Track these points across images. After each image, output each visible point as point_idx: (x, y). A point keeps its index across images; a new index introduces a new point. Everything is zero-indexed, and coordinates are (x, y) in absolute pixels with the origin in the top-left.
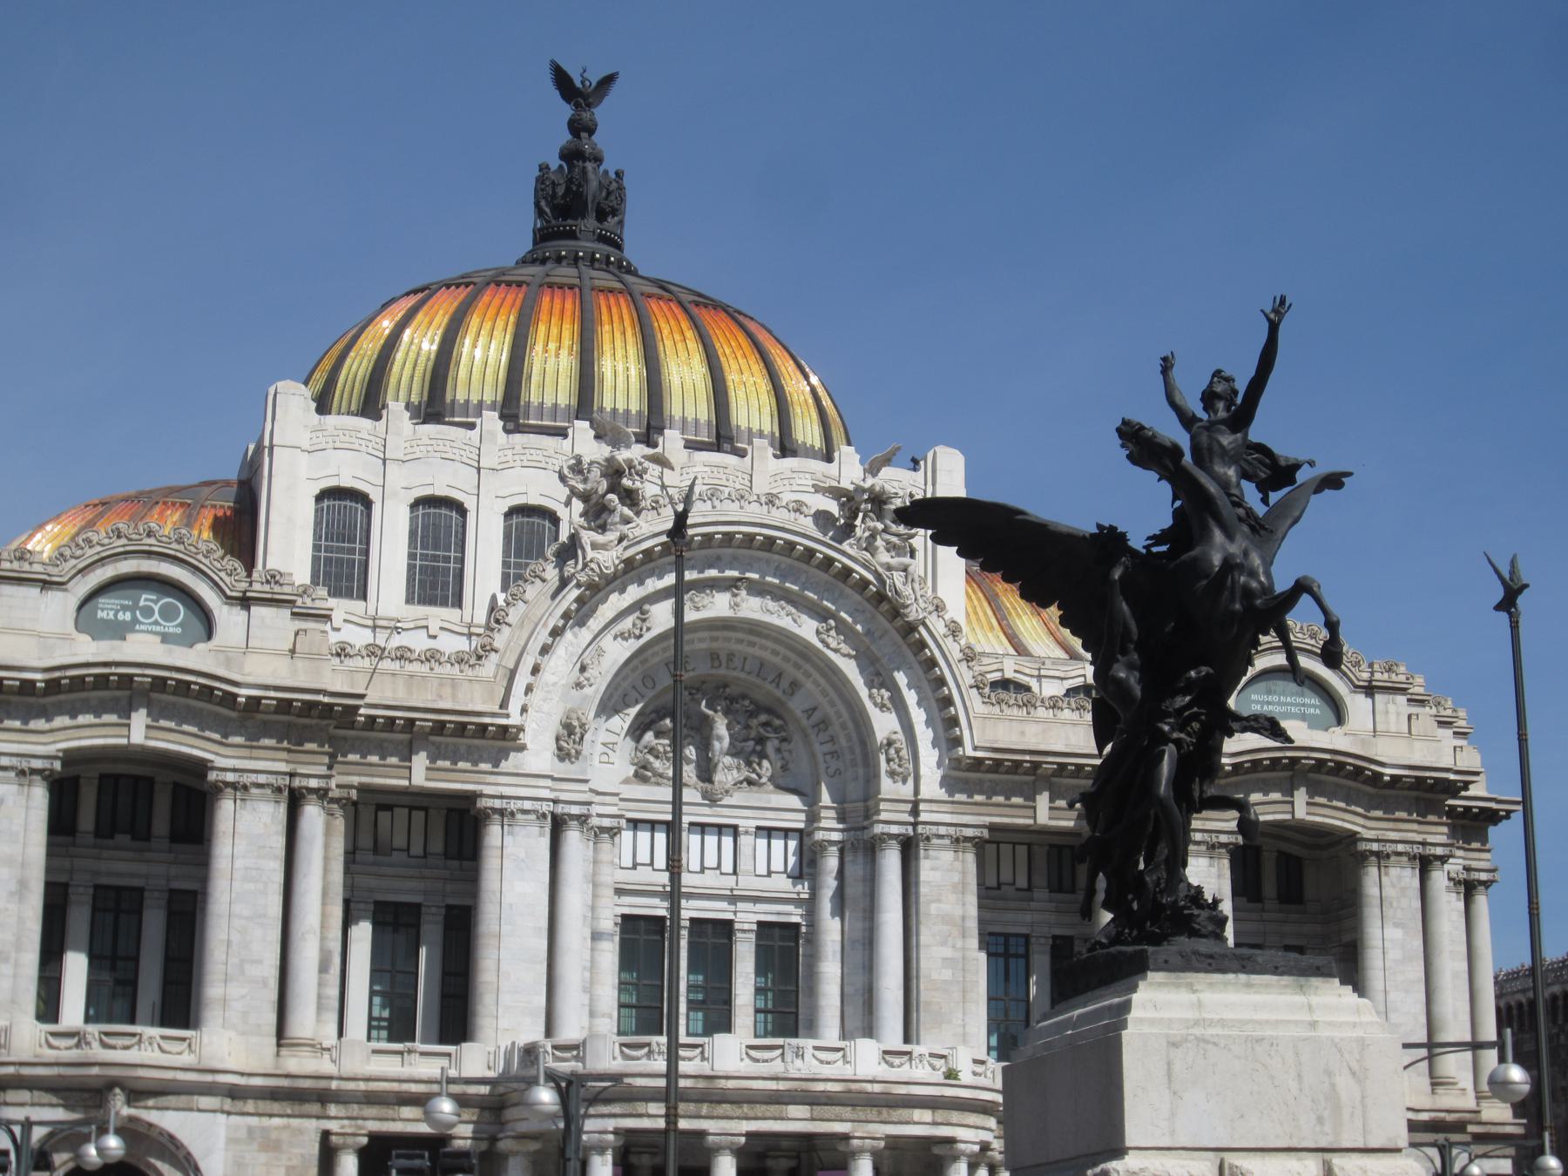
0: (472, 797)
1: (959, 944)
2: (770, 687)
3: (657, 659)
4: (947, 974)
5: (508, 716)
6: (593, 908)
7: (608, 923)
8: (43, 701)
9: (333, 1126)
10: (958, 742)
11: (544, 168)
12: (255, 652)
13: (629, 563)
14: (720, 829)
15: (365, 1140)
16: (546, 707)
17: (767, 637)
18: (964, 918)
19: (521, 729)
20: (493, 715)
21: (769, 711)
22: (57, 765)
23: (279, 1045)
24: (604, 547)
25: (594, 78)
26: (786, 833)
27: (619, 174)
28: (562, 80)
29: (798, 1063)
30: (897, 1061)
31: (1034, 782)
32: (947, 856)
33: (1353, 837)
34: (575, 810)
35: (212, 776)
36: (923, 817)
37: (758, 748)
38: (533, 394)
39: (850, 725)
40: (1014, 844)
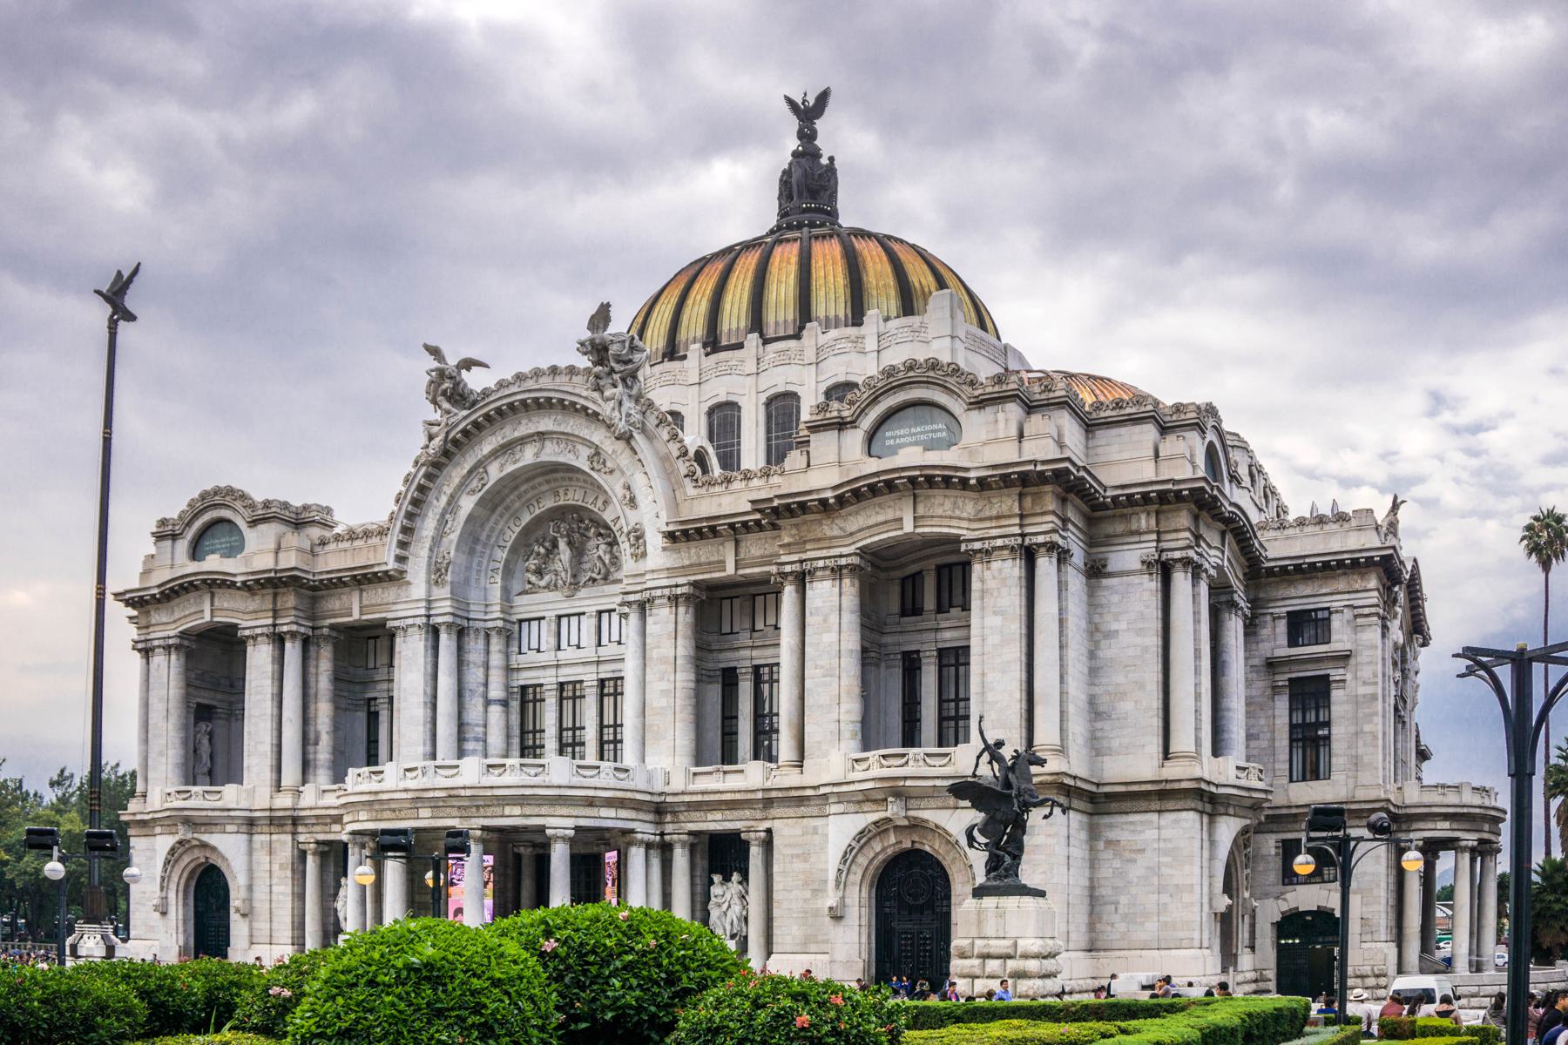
3: (517, 505)
4: (663, 702)
14: (579, 614)
27: (831, 159)
30: (496, 772)
33: (956, 540)
34: (440, 620)
38: (682, 335)
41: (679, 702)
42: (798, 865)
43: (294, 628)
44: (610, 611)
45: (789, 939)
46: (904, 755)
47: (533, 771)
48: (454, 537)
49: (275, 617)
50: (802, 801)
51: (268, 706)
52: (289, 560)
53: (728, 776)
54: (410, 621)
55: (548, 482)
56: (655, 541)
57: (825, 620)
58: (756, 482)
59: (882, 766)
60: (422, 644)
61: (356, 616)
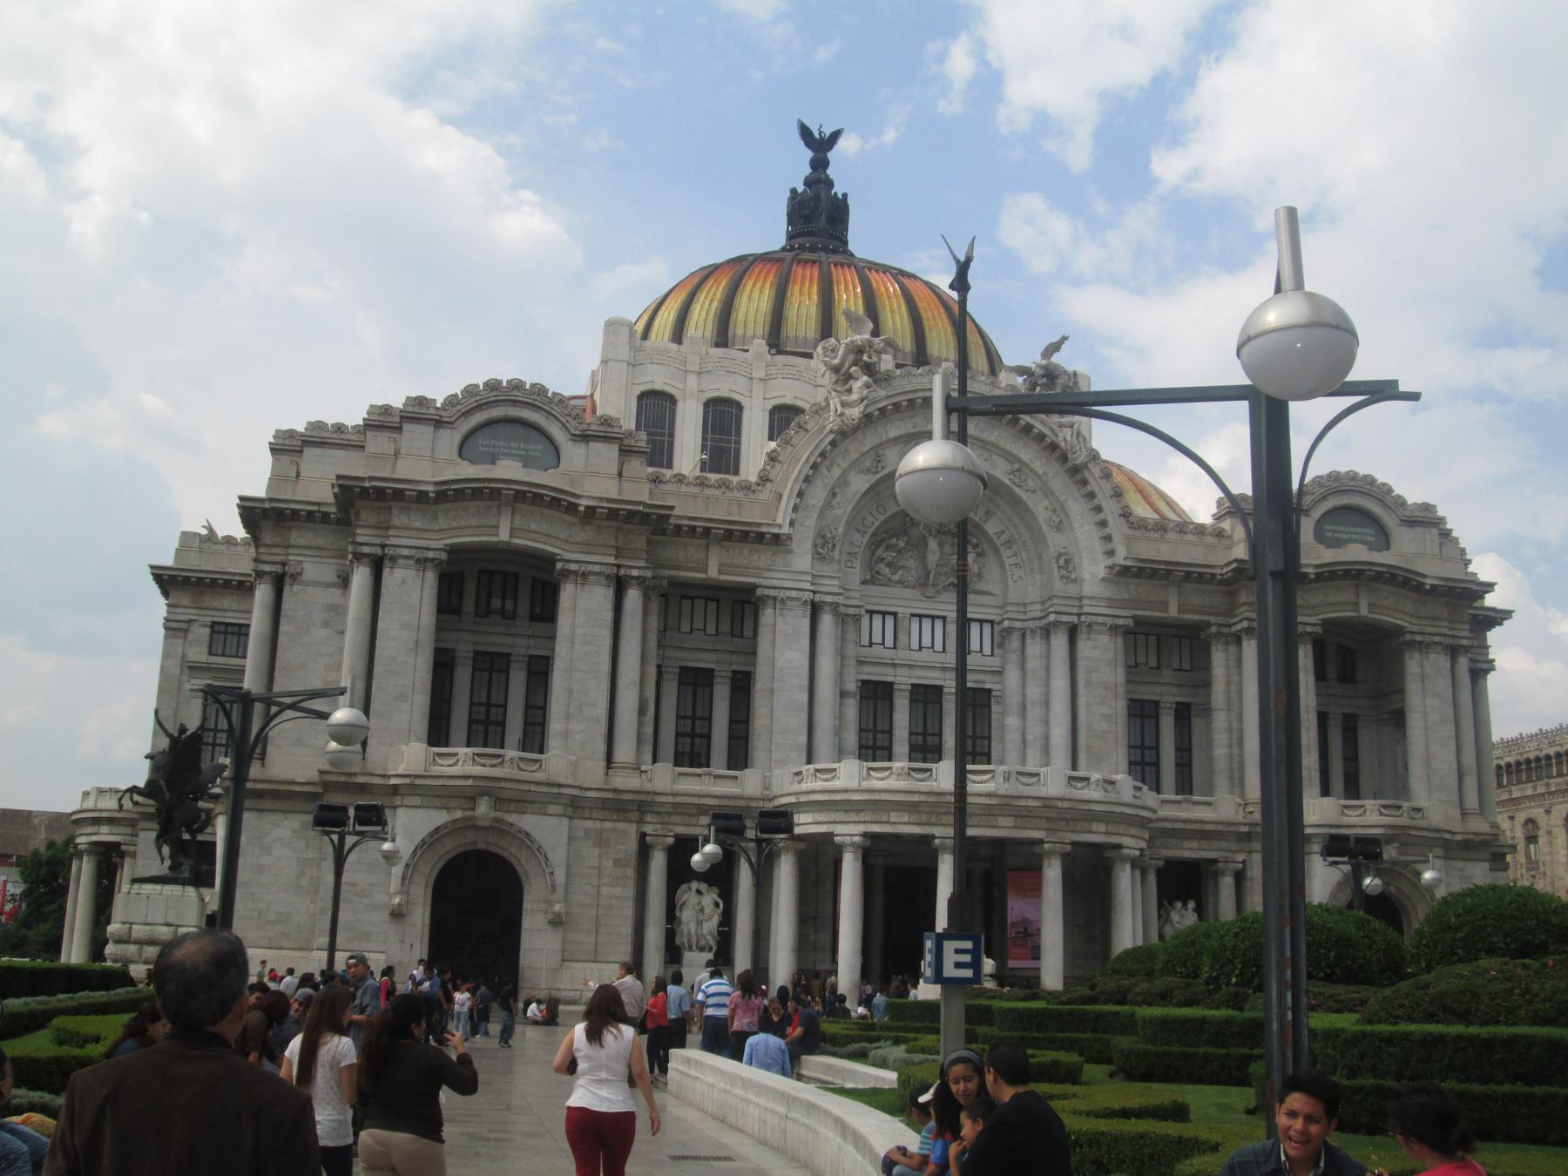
0: (752, 588)
4: (1104, 726)
6: (841, 674)
7: (851, 686)
8: (434, 508)
9: (648, 829)
10: (1111, 553)
11: (794, 191)
12: (591, 475)
13: (868, 418)
14: (933, 618)
15: (671, 841)
19: (789, 537)
22: (444, 556)
23: (608, 768)
25: (827, 132)
27: (845, 196)
28: (805, 133)
30: (1079, 785)
34: (829, 599)
35: (559, 566)
36: (1086, 610)
43: (649, 574)
46: (1399, 807)
47: (1110, 788)
49: (616, 557)
51: (606, 666)
52: (638, 492)
53: (1197, 808)
54: (794, 594)
56: (1093, 571)
58: (1190, 537)
59: (1381, 814)
61: (713, 573)
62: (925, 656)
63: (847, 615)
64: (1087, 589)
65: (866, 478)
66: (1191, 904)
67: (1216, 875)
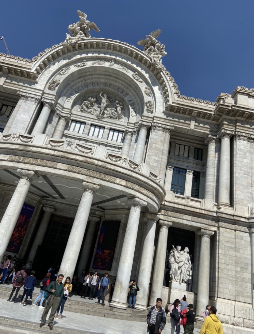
1: (161, 156)
2: (120, 94)
3: (89, 81)
4: (155, 164)
5: (31, 69)
10: (168, 101)
14: (100, 127)
16: (47, 75)
17: (120, 80)
18: (163, 150)
20: (27, 68)
21: (119, 101)
24: (73, 39)
26: (119, 131)
29: (68, 148)
30: (114, 159)
31: (191, 118)
32: (161, 133)
34: (48, 101)
36: (154, 121)
37: (115, 110)
39: (140, 103)
40: (185, 146)
41: (162, 166)
42: (232, 253)
44: (114, 130)
45: (227, 291)
47: (134, 166)
48: (64, 77)
50: (235, 222)
55: (106, 79)
56: (159, 109)
57: (245, 154)
60: (35, 106)
62: (93, 138)
63: (63, 117)
64: (156, 115)
65: (77, 68)
66: (187, 249)
67: (201, 236)
